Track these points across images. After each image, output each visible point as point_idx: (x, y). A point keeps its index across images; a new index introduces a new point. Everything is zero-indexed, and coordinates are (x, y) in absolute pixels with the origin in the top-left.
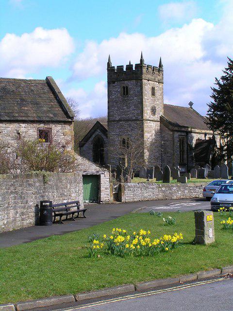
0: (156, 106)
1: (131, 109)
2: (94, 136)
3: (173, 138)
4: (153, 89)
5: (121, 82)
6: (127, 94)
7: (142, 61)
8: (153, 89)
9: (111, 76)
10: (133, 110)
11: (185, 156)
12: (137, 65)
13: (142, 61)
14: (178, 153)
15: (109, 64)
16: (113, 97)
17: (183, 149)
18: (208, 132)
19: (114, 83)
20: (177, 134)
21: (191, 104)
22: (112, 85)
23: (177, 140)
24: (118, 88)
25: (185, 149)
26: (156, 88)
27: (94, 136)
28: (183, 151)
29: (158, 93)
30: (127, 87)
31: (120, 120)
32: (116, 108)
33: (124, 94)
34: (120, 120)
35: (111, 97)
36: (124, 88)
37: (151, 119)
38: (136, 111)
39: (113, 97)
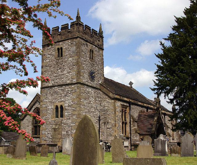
1: (65, 72)
2: (33, 108)
3: (115, 106)
6: (62, 56)
7: (78, 18)
8: (91, 51)
11: (128, 129)
12: (73, 24)
13: (78, 18)
14: (121, 124)
17: (125, 120)
18: (149, 106)
19: (48, 45)
20: (119, 104)
21: (131, 83)
22: (46, 48)
23: (119, 109)
24: (52, 51)
25: (128, 120)
27: (33, 108)
28: (126, 124)
29: (97, 59)
30: (62, 48)
31: (54, 86)
34: (54, 86)
36: (58, 49)
37: (89, 84)
38: (71, 74)
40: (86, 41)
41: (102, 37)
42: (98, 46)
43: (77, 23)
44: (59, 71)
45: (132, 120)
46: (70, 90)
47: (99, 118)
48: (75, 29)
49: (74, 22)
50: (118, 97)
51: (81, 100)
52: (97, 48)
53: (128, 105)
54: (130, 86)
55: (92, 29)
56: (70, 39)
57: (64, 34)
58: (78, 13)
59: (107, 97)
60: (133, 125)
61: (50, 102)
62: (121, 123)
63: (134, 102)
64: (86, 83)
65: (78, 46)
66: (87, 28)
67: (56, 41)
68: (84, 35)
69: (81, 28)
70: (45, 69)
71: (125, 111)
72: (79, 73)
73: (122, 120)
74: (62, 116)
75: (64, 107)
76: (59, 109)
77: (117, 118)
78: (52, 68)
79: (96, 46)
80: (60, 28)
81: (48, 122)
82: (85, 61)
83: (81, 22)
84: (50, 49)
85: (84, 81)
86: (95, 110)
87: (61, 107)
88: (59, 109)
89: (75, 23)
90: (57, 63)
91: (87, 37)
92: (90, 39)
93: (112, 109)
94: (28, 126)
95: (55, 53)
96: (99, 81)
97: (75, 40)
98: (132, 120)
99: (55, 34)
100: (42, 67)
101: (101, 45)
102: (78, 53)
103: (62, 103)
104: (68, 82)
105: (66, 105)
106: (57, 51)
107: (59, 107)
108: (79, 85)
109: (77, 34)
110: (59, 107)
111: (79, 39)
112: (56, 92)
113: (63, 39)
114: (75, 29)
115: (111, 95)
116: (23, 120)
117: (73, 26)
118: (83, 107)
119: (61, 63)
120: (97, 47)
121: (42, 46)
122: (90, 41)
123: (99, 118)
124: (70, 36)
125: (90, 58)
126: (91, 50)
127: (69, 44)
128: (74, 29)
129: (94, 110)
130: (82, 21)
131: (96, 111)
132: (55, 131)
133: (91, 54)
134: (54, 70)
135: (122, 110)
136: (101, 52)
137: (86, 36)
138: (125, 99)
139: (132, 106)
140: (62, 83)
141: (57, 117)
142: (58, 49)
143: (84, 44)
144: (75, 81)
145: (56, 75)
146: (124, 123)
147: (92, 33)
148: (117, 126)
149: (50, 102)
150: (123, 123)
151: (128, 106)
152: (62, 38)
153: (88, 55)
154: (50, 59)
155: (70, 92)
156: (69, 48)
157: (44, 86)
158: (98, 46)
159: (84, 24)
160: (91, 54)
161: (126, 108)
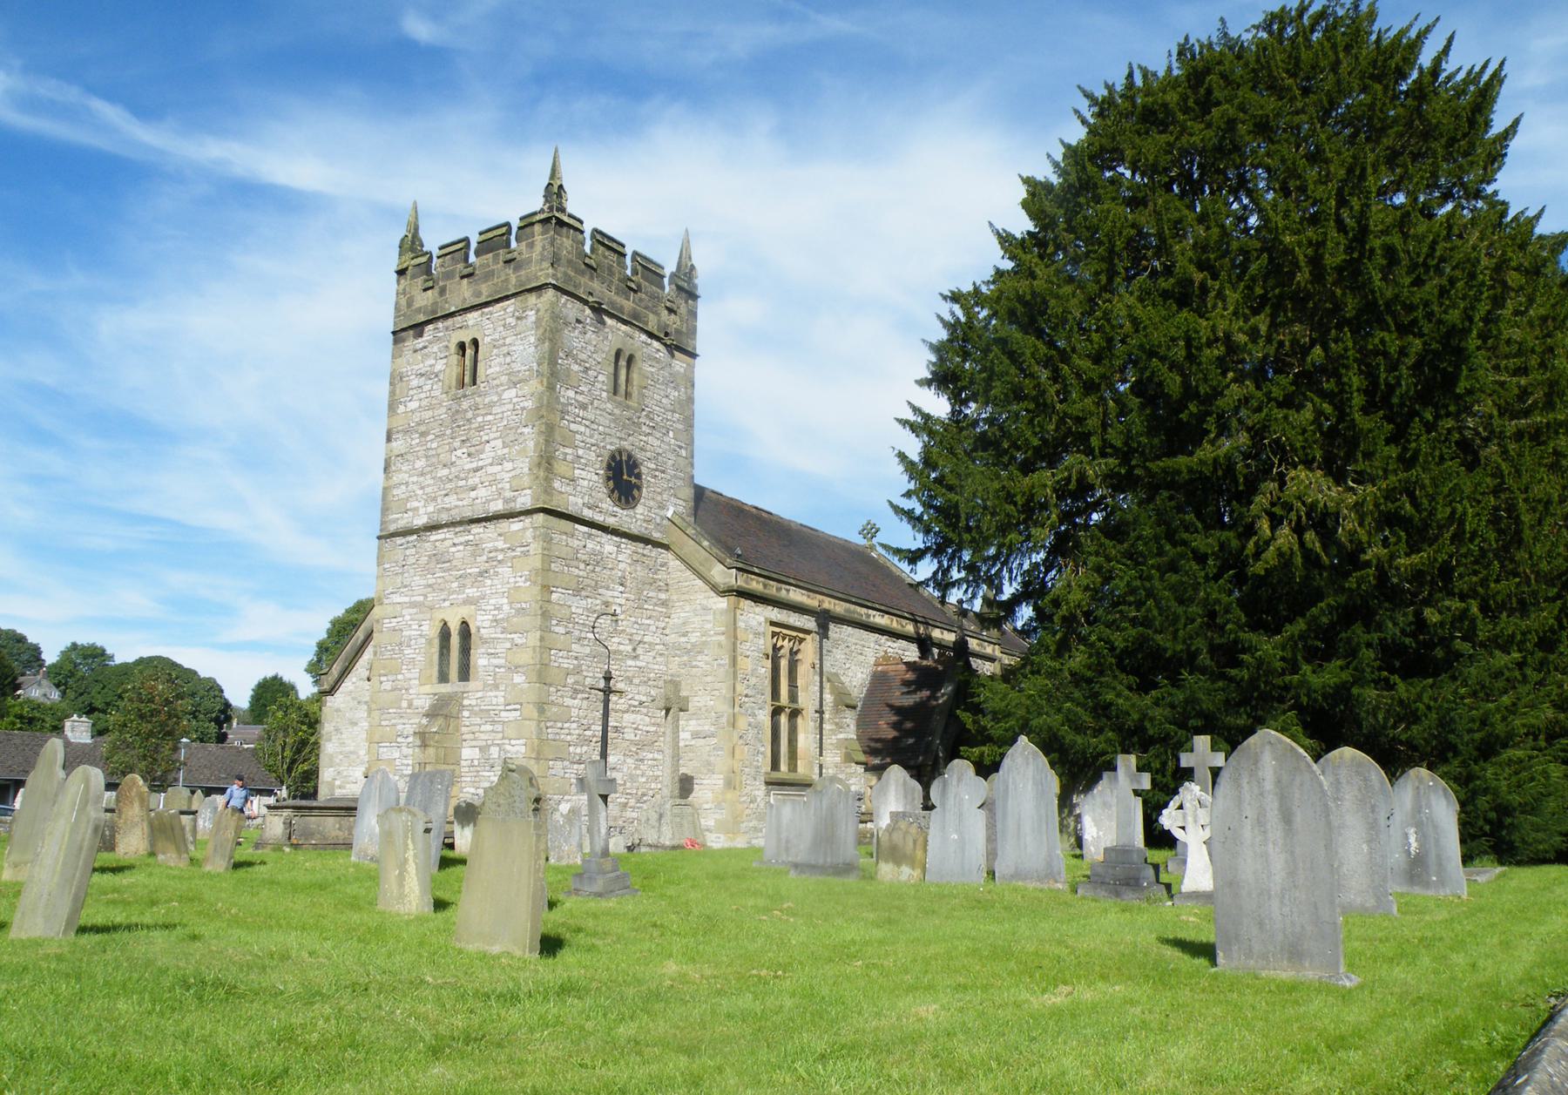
0: (639, 455)
1: (487, 456)
4: (623, 360)
5: (449, 322)
7: (555, 193)
8: (623, 360)
9: (410, 304)
10: (500, 461)
12: (528, 223)
13: (555, 193)
14: (764, 717)
15: (411, 244)
16: (413, 405)
17: (793, 697)
19: (418, 329)
20: (756, 617)
22: (412, 343)
23: (756, 645)
25: (807, 700)
26: (644, 367)
29: (659, 399)
30: (475, 342)
31: (433, 527)
32: (420, 464)
33: (462, 385)
34: (433, 527)
35: (401, 409)
36: (462, 347)
37: (599, 518)
38: (508, 466)
39: (413, 405)
40: (598, 310)
41: (692, 295)
42: (667, 334)
43: (542, 216)
44: (459, 453)
45: (828, 697)
46: (500, 545)
47: (608, 678)
48: (538, 248)
49: (535, 214)
50: (756, 585)
51: (554, 596)
52: (656, 344)
53: (809, 623)
54: (860, 541)
55: (635, 254)
56: (514, 295)
57: (489, 276)
58: (554, 172)
59: (699, 582)
60: (837, 724)
61: (413, 605)
62: (768, 709)
63: (847, 610)
64: (588, 514)
65: (552, 334)
66: (603, 244)
67: (453, 309)
68: (584, 280)
69: (566, 242)
70: (398, 445)
71: (793, 653)
72: (546, 462)
73: (775, 694)
74: (465, 674)
75: (473, 630)
76: (455, 641)
77: (740, 688)
78: (429, 438)
79: (651, 335)
80: (474, 245)
81: (404, 704)
82: (584, 407)
83: (570, 216)
84: (425, 347)
85: (574, 503)
86: (634, 650)
87: (465, 624)
88: (455, 641)
89: (538, 217)
90: (455, 414)
91: (599, 289)
92: (620, 300)
93: (720, 645)
94: (355, 724)
95: (446, 365)
96: (662, 507)
97: (532, 299)
98: (828, 697)
99: (448, 276)
100: (389, 439)
101: (678, 332)
102: (553, 372)
103: (465, 612)
104: (498, 506)
105: (481, 623)
106: (455, 359)
107: (454, 627)
108: (540, 517)
109: (545, 274)
110: (454, 627)
111: (551, 292)
112: (439, 558)
113: (483, 299)
114: (538, 248)
115: (723, 574)
116: (331, 691)
117: (528, 230)
118: (561, 630)
119: (469, 415)
120: (658, 339)
121: (394, 333)
122: (621, 309)
123: (608, 678)
124: (513, 280)
125: (615, 393)
126: (618, 354)
127: (509, 320)
128: (531, 246)
129: (629, 648)
130: (573, 205)
131: (639, 651)
132: (424, 745)
133: (623, 373)
134: (439, 451)
135: (776, 649)
136: (680, 363)
137: (596, 285)
138: (796, 595)
139: (834, 630)
140: (468, 514)
141: (443, 678)
142: (462, 347)
143: (578, 321)
144: (525, 500)
145: (445, 472)
146: (784, 712)
147: (635, 272)
148: (742, 723)
149: (413, 605)
150: (776, 712)
151: (808, 632)
152: (478, 294)
153: (601, 378)
154: (423, 395)
155: (500, 557)
156: (508, 341)
157: (392, 528)
158: (667, 334)
159: (588, 228)
160: (623, 373)
161: (801, 641)
